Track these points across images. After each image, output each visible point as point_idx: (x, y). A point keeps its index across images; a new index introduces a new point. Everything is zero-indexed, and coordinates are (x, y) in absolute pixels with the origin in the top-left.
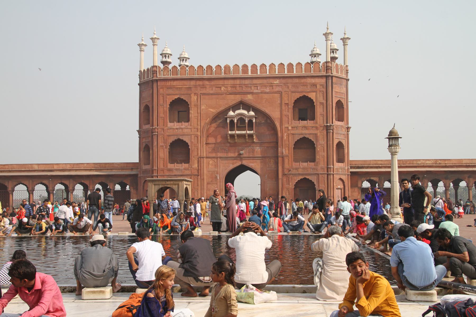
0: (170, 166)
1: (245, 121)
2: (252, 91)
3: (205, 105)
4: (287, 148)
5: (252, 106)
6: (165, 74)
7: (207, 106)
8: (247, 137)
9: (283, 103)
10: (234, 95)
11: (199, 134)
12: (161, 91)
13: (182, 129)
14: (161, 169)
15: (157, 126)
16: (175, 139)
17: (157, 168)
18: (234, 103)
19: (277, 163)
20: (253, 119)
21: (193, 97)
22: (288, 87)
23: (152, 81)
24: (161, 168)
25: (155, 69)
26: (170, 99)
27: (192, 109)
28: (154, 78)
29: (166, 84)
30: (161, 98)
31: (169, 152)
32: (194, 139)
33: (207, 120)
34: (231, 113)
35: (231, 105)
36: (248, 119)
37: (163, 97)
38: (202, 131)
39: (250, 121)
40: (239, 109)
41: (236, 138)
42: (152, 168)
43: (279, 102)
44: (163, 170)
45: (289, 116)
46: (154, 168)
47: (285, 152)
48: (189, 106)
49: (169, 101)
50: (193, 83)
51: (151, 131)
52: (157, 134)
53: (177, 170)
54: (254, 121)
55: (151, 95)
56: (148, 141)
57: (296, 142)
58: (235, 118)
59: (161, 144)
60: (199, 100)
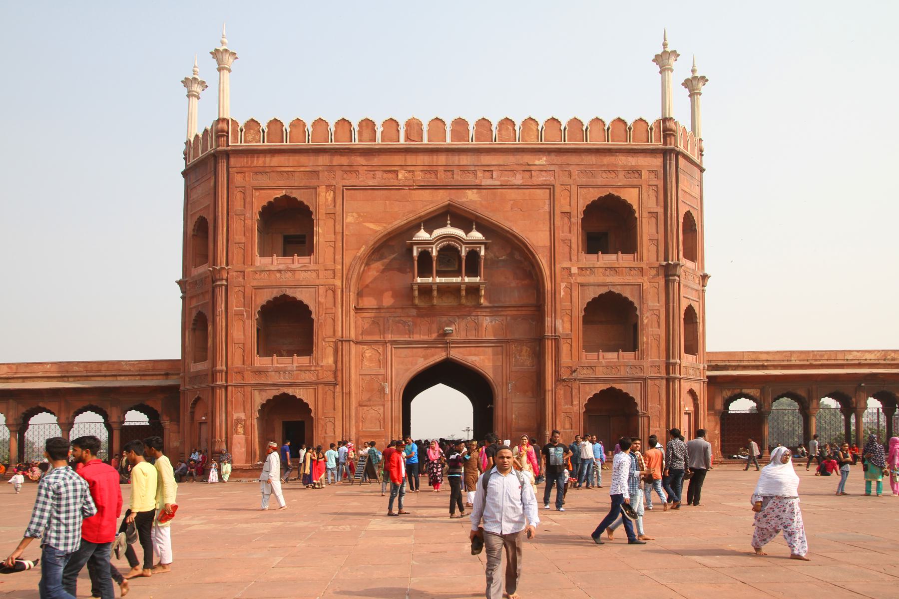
0: (261, 362)
1: (457, 252)
2: (477, 182)
3: (354, 214)
4: (566, 319)
5: (477, 217)
6: (250, 138)
7: (360, 216)
8: (463, 293)
9: (557, 212)
10: (431, 191)
11: (338, 283)
12: (238, 179)
13: (293, 271)
14: (235, 370)
15: (227, 265)
16: (273, 296)
17: (224, 368)
18: (432, 209)
19: (539, 356)
20: (480, 248)
21: (323, 194)
22: (570, 175)
23: (215, 156)
24: (237, 368)
25: (223, 125)
26: (260, 200)
27: (321, 223)
28: (220, 148)
29: (252, 162)
30: (238, 196)
31: (258, 330)
32: (326, 296)
33: (359, 249)
34: (422, 235)
35: (422, 214)
36: (466, 248)
37: (242, 195)
38: (347, 276)
39: (473, 255)
40: (445, 225)
41: (435, 293)
42: (213, 367)
43: (547, 208)
44: (241, 372)
45: (573, 241)
46: (219, 368)
47: (563, 327)
48: (313, 217)
49: (257, 207)
50: (323, 160)
51: (210, 279)
52: (224, 283)
53: (278, 371)
54: (482, 253)
55: (212, 191)
56: (202, 304)
57: (589, 304)
58: (434, 246)
59: (235, 308)
60: (339, 201)
